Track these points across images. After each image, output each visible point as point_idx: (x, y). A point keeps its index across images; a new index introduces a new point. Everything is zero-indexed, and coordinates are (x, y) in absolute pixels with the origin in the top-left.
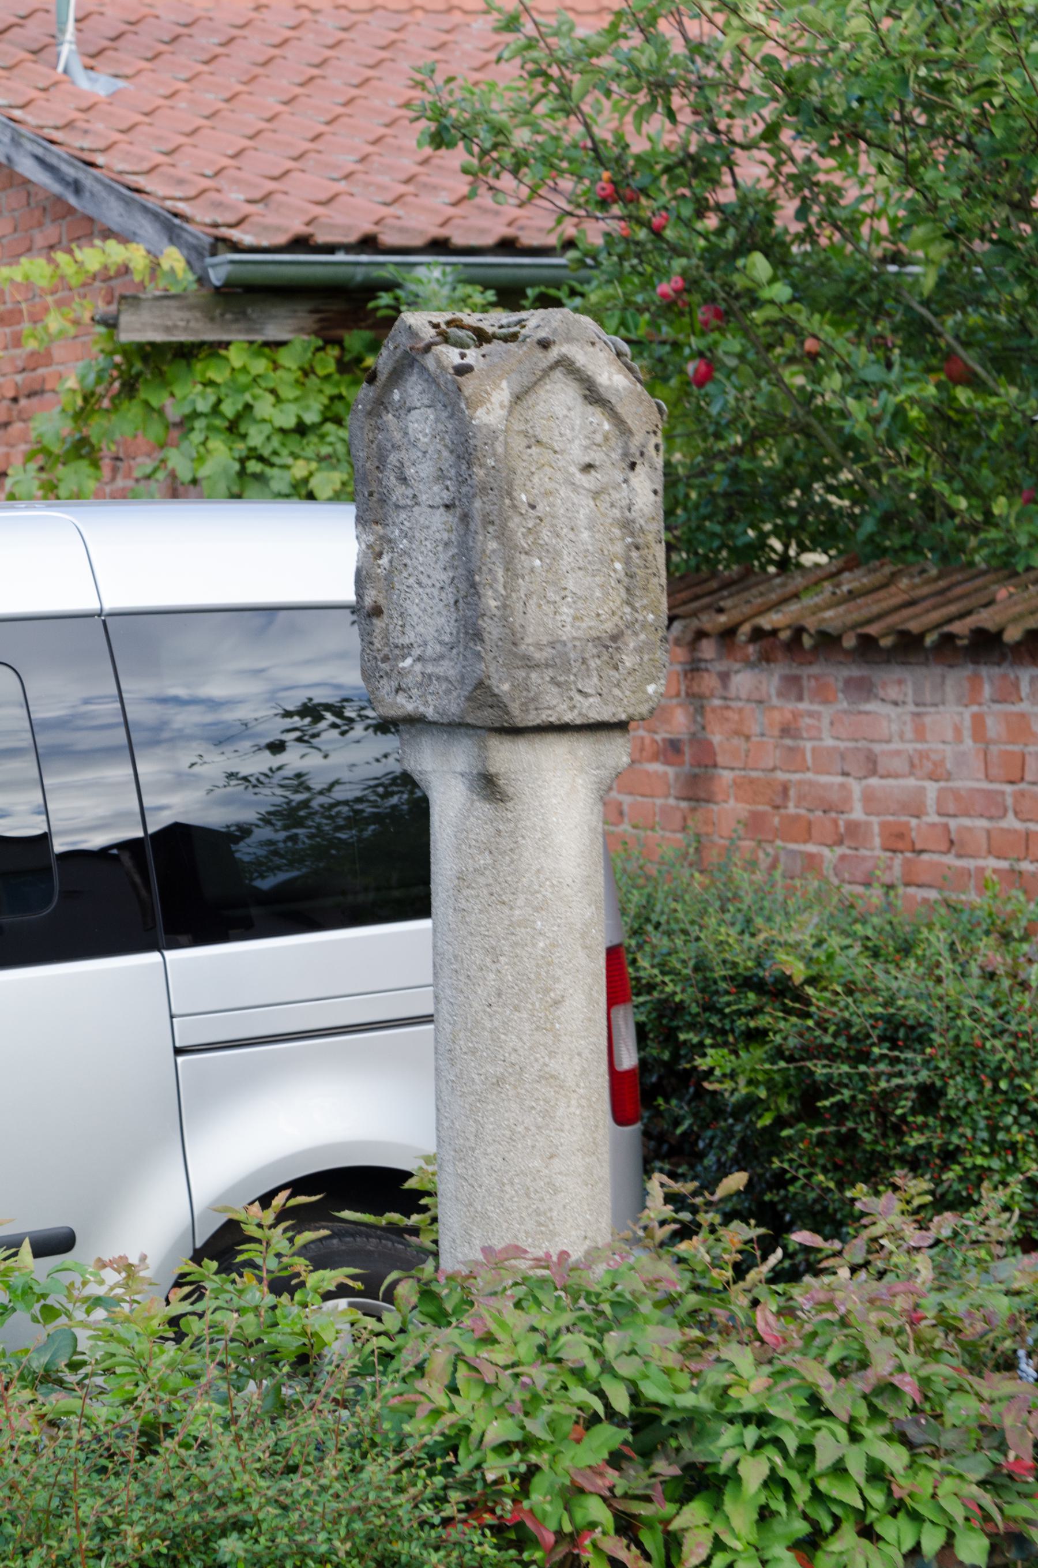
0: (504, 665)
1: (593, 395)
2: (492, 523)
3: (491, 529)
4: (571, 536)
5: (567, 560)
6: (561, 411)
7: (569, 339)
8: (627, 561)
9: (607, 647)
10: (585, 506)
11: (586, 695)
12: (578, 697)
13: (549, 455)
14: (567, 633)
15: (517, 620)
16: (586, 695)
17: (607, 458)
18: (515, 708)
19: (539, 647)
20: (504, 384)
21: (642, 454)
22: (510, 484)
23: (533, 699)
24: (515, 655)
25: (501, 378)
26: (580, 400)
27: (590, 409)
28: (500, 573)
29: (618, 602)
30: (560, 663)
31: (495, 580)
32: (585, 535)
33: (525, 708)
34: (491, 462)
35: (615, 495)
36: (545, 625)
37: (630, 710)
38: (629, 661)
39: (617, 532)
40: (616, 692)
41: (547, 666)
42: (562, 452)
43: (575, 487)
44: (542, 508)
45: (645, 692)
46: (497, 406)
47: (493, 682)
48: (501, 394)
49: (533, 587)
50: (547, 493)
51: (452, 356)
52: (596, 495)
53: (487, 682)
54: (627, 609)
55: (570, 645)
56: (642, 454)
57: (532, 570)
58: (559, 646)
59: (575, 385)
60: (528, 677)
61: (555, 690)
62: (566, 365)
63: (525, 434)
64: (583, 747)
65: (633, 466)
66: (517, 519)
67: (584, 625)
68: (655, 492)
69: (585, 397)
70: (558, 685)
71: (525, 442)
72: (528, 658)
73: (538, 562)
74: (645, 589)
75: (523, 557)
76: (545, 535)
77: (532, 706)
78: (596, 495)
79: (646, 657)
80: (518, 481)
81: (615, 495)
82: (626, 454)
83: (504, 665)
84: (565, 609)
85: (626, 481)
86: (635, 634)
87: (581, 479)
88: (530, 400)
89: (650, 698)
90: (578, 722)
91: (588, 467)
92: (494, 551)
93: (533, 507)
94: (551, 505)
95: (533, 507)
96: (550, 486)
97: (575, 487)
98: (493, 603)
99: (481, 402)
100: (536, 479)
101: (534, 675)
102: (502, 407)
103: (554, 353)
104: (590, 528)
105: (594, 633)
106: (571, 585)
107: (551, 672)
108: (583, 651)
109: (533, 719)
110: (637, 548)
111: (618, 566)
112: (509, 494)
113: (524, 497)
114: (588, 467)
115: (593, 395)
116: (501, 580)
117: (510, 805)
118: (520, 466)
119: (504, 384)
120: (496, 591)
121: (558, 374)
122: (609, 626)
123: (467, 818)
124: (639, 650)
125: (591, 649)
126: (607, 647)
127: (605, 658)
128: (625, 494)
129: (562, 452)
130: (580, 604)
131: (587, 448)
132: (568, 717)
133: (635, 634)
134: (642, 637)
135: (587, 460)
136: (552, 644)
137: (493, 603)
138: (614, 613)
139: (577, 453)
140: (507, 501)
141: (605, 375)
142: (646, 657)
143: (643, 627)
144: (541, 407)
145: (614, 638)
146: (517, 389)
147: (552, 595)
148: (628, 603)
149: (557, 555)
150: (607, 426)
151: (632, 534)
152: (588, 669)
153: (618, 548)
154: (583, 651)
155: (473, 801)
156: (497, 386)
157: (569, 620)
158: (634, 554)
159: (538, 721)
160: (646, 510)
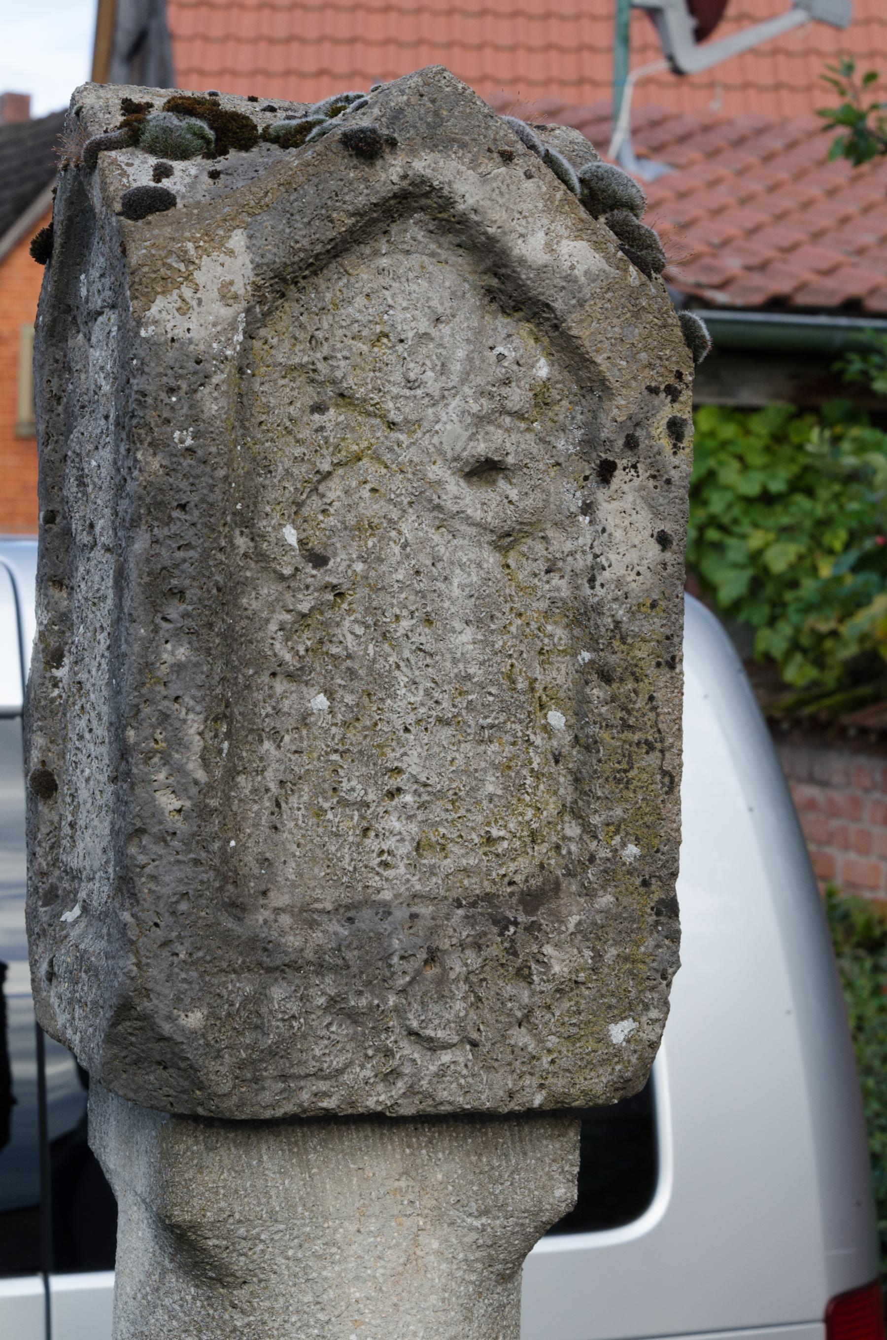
0: (191, 963)
1: (508, 290)
2: (180, 594)
3: (174, 610)
4: (424, 636)
5: (405, 700)
6: (410, 322)
7: (436, 139)
8: (579, 709)
9: (502, 924)
10: (468, 567)
11: (433, 1046)
12: (408, 1049)
13: (370, 433)
14: (396, 883)
15: (252, 844)
16: (433, 1046)
17: (544, 452)
18: (220, 1075)
19: (307, 916)
20: (238, 240)
21: (631, 443)
22: (253, 498)
23: (272, 1053)
24: (227, 938)
25: (230, 223)
26: (473, 300)
27: (502, 324)
28: (193, 727)
29: (552, 809)
30: (366, 958)
31: (178, 742)
32: (465, 638)
33: (249, 1072)
34: (183, 438)
35: (561, 543)
36: (330, 861)
37: (559, 1084)
38: (560, 962)
39: (559, 633)
40: (521, 1037)
41: (321, 968)
42: (412, 425)
43: (445, 519)
44: (344, 562)
45: (603, 1039)
46: (211, 294)
47: (157, 1005)
48: (228, 267)
49: (302, 764)
50: (365, 528)
51: (137, 170)
52: (505, 539)
53: (145, 1005)
54: (573, 830)
55: (400, 914)
56: (631, 443)
57: (304, 719)
58: (366, 918)
59: (461, 261)
60: (260, 997)
61: (341, 1030)
62: (417, 200)
63: (309, 372)
64: (446, 1167)
65: (606, 471)
66: (268, 589)
67: (448, 864)
68: (663, 540)
69: (491, 294)
70: (353, 1016)
71: (310, 395)
72: (268, 947)
73: (320, 702)
74: (622, 780)
75: (280, 686)
76: (349, 633)
77: (270, 1070)
78: (505, 539)
79: (611, 953)
80: (277, 491)
81: (561, 543)
82: (590, 443)
83: (191, 963)
84: (394, 823)
85: (588, 508)
86: (589, 893)
87: (457, 492)
88: (329, 288)
89: (618, 1052)
90: (407, 1110)
91: (485, 470)
92: (179, 668)
93: (319, 560)
94: (371, 558)
95: (319, 560)
96: (371, 509)
97: (445, 519)
98: (168, 802)
99: (168, 283)
100: (334, 490)
101: (278, 992)
102: (226, 296)
103: (392, 171)
104: (481, 620)
105: (475, 885)
106: (413, 763)
107: (329, 985)
108: (433, 931)
109: (270, 1100)
110: (606, 677)
111: (556, 718)
112: (246, 522)
113: (291, 535)
114: (485, 470)
115: (508, 290)
116: (197, 744)
117: (241, 1294)
118: (286, 455)
119: (238, 240)
120: (180, 770)
121: (412, 230)
122: (521, 868)
123: (152, 1308)
124: (592, 934)
125: (457, 927)
126: (502, 924)
127: (494, 951)
128: (585, 540)
129: (412, 425)
130: (438, 811)
131: (481, 420)
132: (377, 1099)
133: (589, 893)
134: (605, 900)
135: (481, 448)
136: (347, 912)
137: (168, 802)
138: (534, 837)
139: (451, 428)
140: (242, 543)
141: (538, 240)
142: (611, 953)
143: (609, 876)
144: (357, 308)
145: (532, 900)
146: (277, 255)
147: (353, 785)
148: (578, 815)
149: (379, 685)
150: (543, 370)
151: (593, 644)
152: (441, 981)
153: (560, 674)
154: (433, 931)
155: (164, 1272)
156: (214, 241)
157: (405, 848)
158: (597, 692)
159: (288, 1108)
160: (634, 586)
